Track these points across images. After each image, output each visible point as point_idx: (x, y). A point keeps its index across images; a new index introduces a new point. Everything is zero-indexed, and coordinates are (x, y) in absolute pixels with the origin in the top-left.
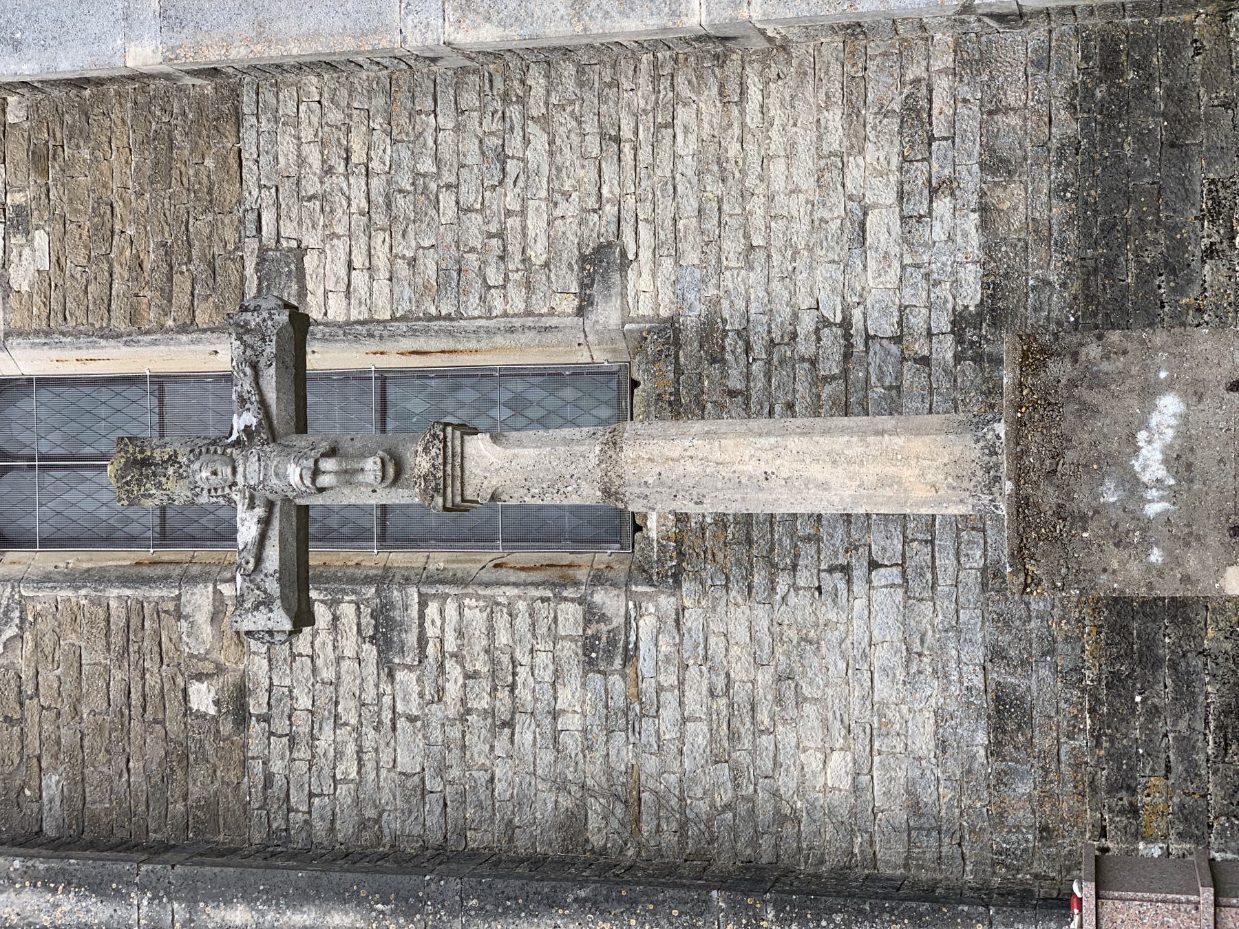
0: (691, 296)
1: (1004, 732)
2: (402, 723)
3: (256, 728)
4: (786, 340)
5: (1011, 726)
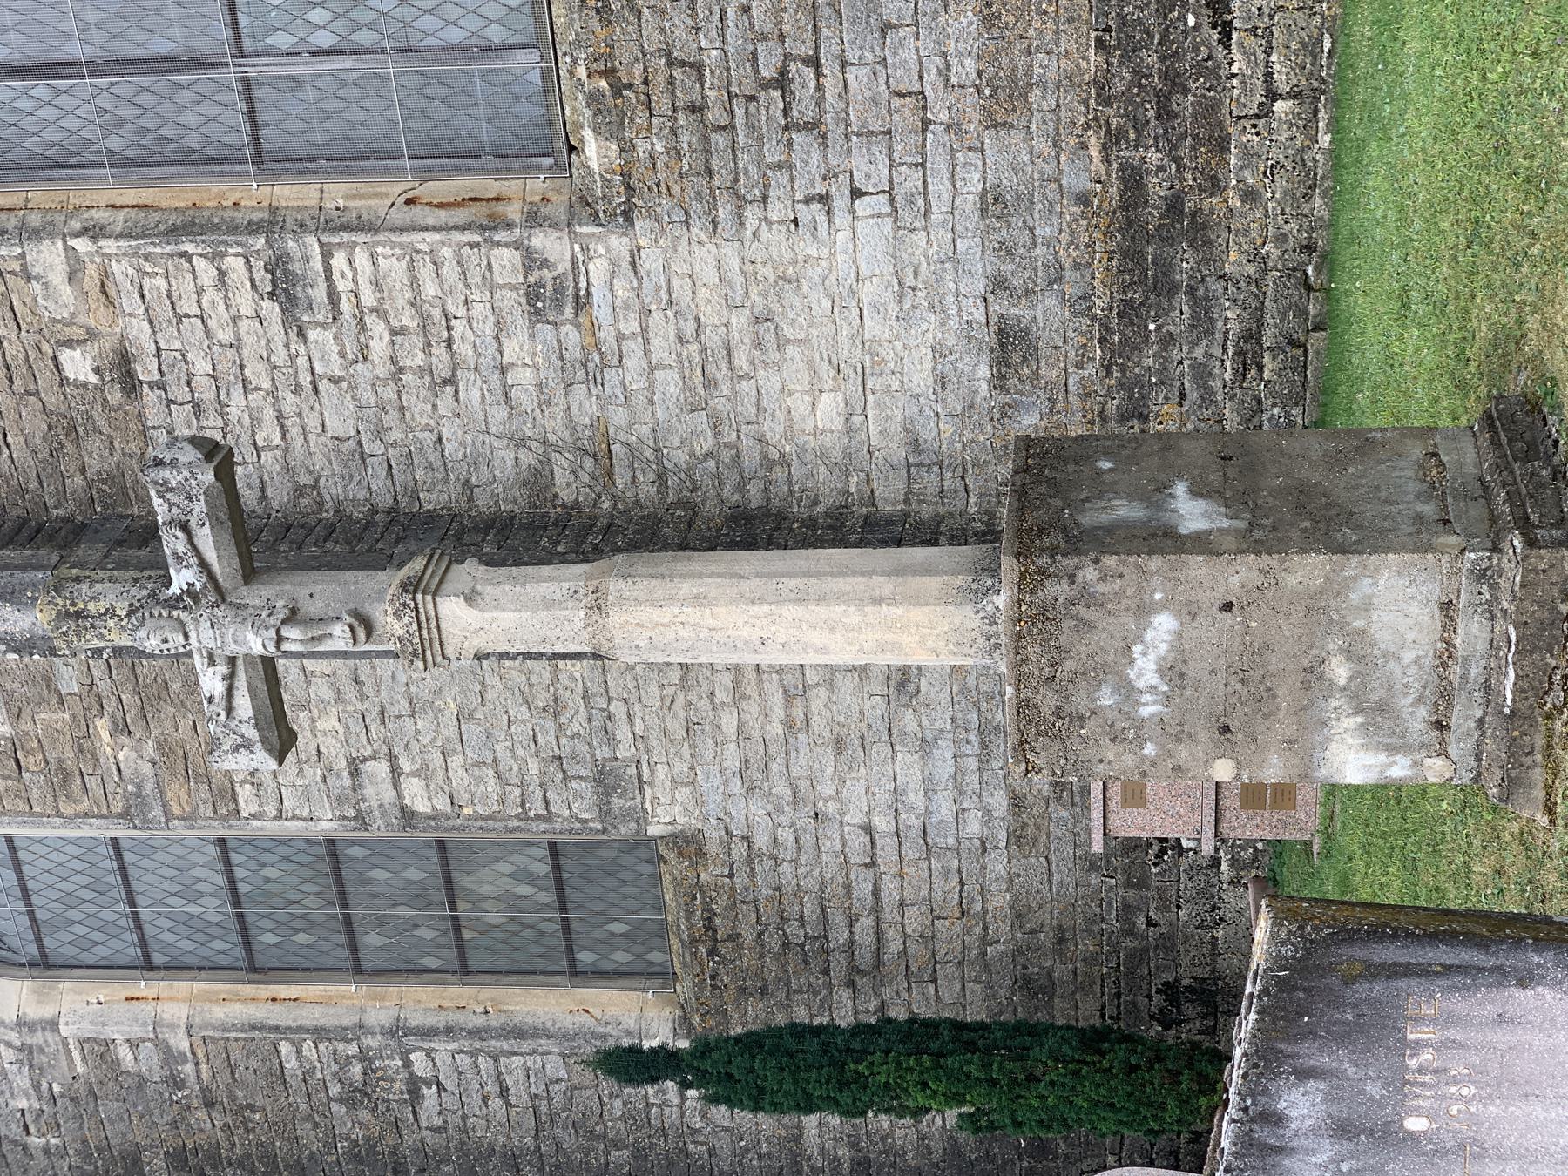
1: (1008, 365)
2: (323, 386)
3: (150, 397)
5: (1015, 358)
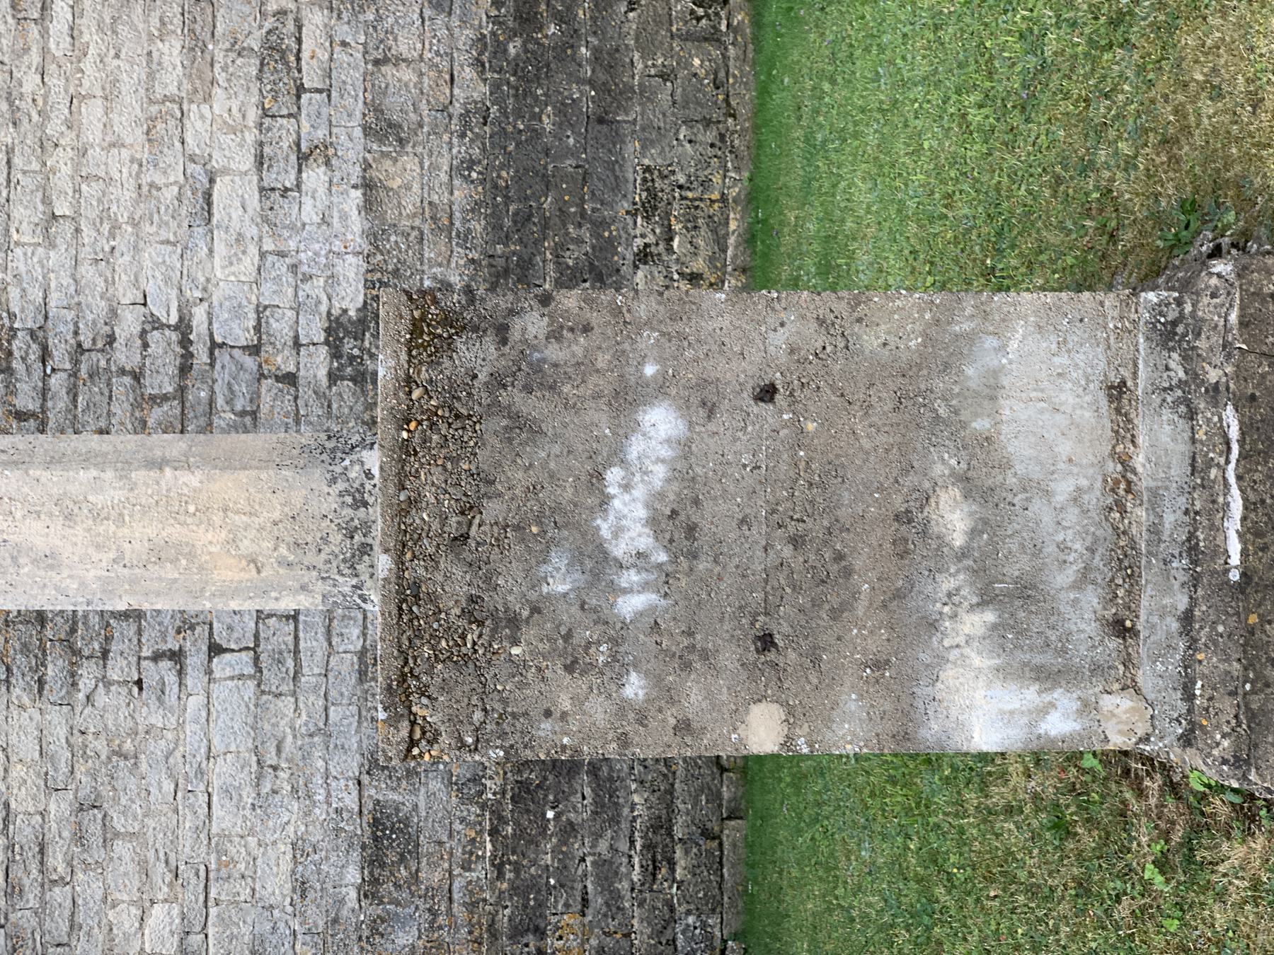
1: (382, 865)
4: (100, 345)
5: (392, 857)
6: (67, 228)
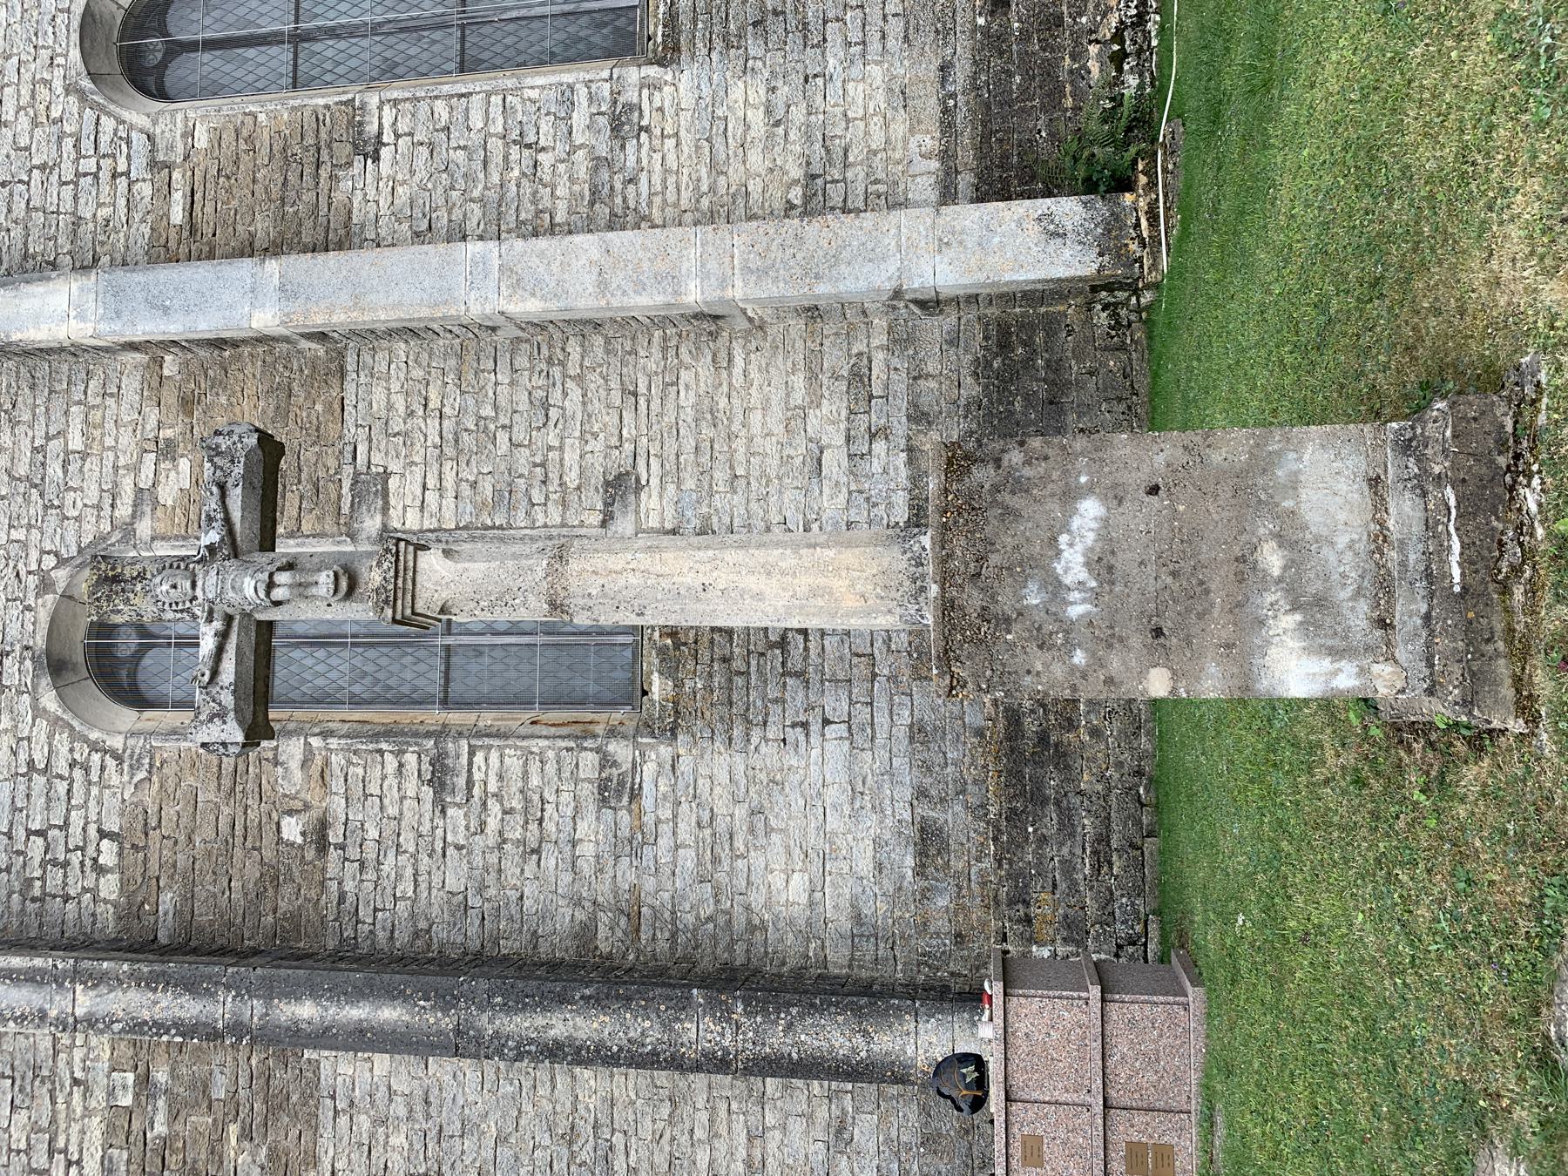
0: (689, 513)
1: (927, 856)
2: (450, 851)
3: (333, 854)
5: (933, 851)
6: (743, 482)
